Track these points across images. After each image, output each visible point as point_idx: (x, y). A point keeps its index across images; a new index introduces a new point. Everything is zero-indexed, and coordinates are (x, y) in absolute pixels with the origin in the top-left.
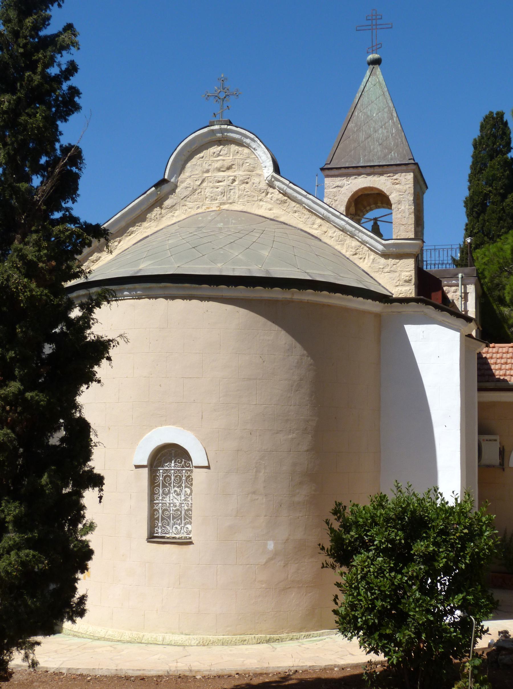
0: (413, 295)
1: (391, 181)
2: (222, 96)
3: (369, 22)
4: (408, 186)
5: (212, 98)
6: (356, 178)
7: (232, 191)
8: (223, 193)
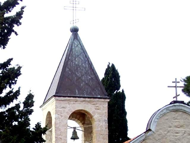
1: (95, 107)
3: (72, 5)
4: (104, 111)
6: (74, 103)
7: (184, 139)
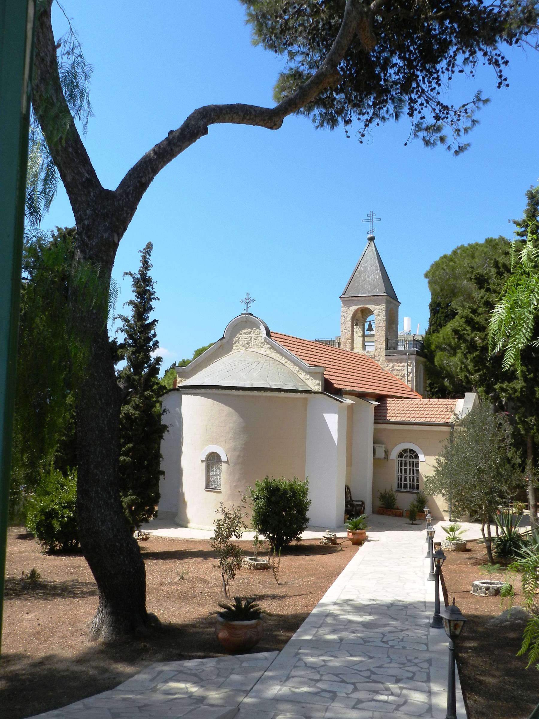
0: (320, 391)
2: (248, 301)
5: (243, 302)
8: (247, 344)
